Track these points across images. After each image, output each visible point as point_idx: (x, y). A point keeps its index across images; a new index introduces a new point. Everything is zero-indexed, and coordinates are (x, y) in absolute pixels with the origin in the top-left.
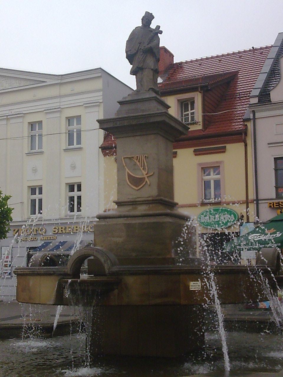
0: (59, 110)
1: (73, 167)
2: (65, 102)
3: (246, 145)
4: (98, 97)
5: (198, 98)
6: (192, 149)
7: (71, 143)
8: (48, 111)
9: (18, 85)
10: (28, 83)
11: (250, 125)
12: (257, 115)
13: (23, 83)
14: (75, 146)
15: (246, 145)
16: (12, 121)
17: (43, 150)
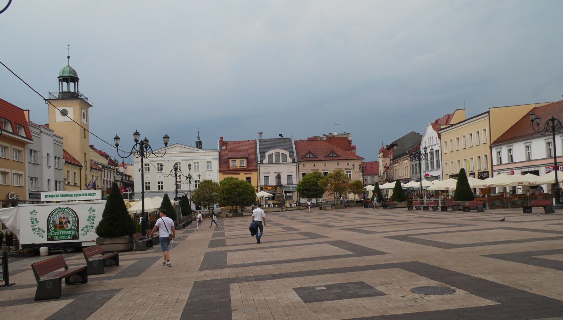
0: (205, 159)
1: (210, 175)
2: (206, 157)
3: (257, 173)
4: (217, 157)
5: (245, 160)
6: (244, 173)
7: (208, 168)
8: (201, 160)
9: (189, 151)
10: (194, 151)
11: (258, 168)
12: (260, 166)
13: (192, 150)
14: (209, 170)
15: (257, 173)
16: (188, 161)
17: (199, 170)
